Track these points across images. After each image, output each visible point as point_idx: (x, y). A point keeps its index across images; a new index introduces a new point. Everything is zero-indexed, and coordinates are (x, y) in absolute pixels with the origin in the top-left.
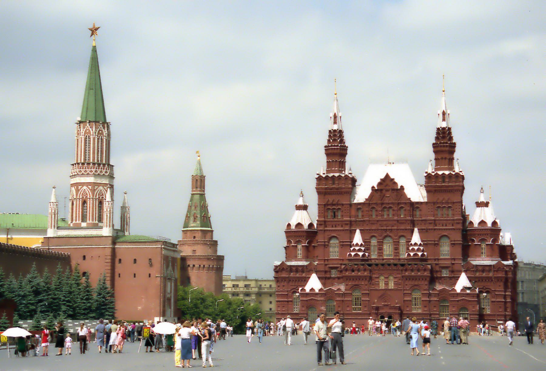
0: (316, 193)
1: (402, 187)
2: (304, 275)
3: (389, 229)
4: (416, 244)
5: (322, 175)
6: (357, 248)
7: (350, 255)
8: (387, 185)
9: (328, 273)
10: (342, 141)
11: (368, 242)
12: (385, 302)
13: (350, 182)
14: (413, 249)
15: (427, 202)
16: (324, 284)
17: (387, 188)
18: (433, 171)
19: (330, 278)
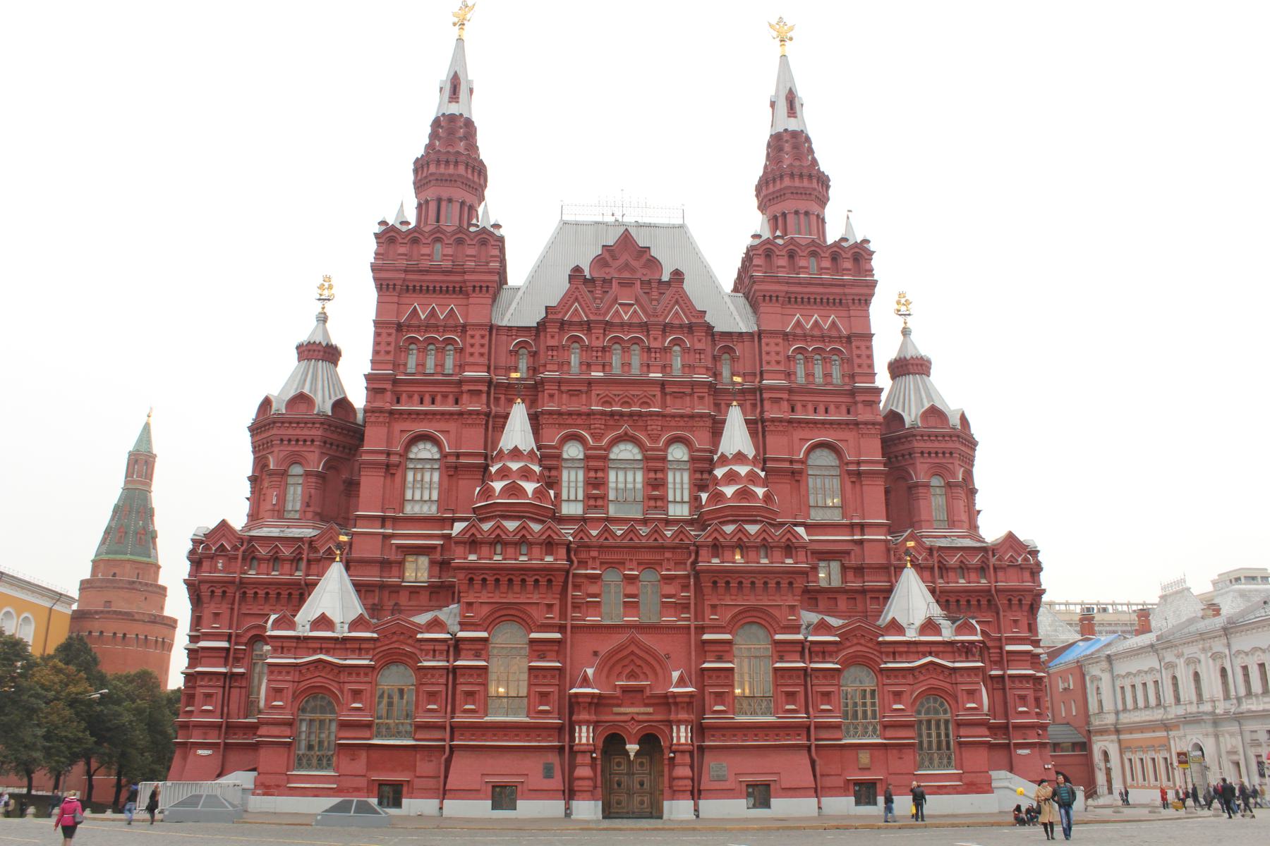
0: (372, 285)
1: (678, 275)
2: (299, 574)
3: (631, 414)
4: (740, 457)
5: (398, 226)
6: (515, 466)
7: (487, 492)
8: (627, 266)
9: (395, 571)
10: (473, 147)
11: (550, 469)
12: (632, 675)
13: (496, 252)
14: (731, 477)
15: (760, 334)
16: (374, 609)
17: (626, 275)
18: (778, 233)
19: (396, 589)
